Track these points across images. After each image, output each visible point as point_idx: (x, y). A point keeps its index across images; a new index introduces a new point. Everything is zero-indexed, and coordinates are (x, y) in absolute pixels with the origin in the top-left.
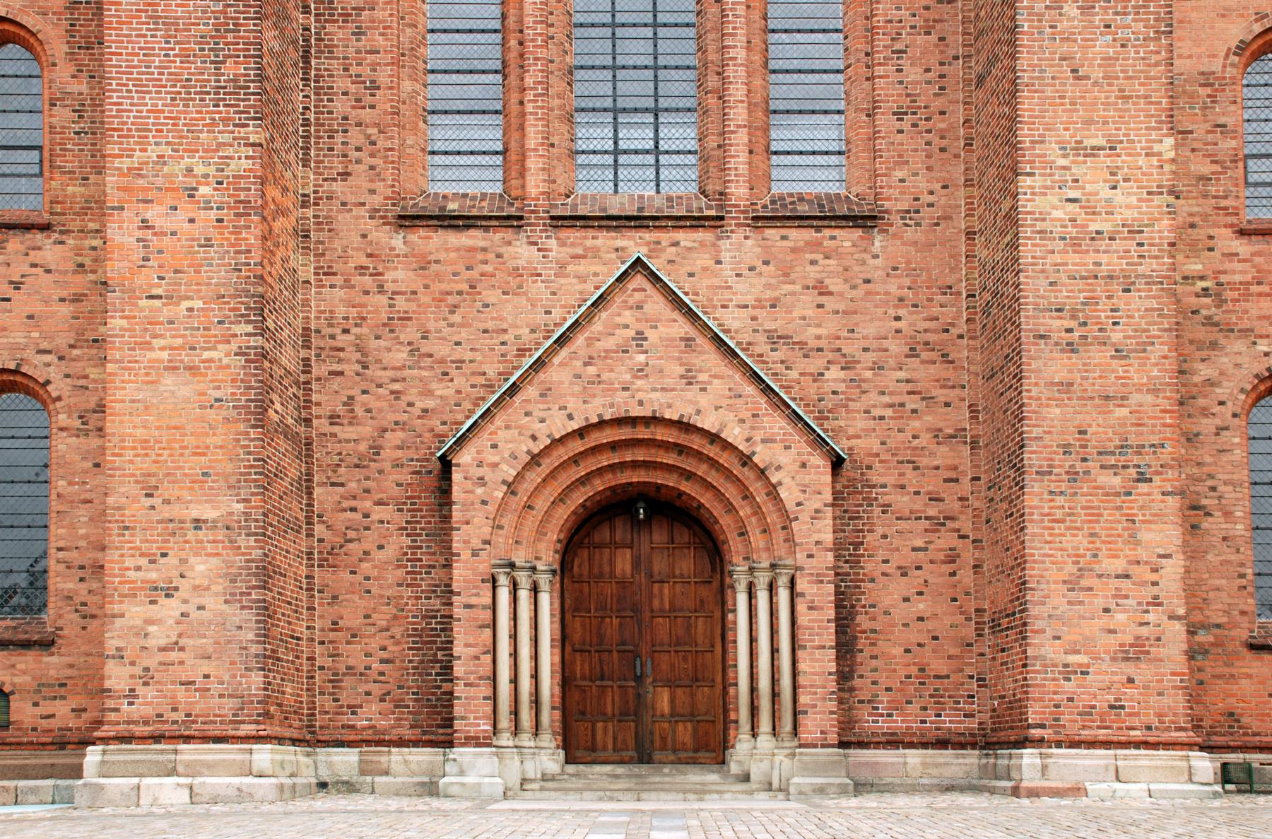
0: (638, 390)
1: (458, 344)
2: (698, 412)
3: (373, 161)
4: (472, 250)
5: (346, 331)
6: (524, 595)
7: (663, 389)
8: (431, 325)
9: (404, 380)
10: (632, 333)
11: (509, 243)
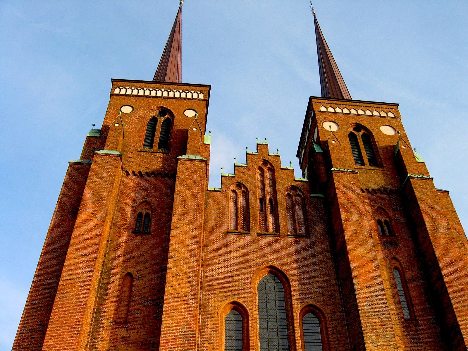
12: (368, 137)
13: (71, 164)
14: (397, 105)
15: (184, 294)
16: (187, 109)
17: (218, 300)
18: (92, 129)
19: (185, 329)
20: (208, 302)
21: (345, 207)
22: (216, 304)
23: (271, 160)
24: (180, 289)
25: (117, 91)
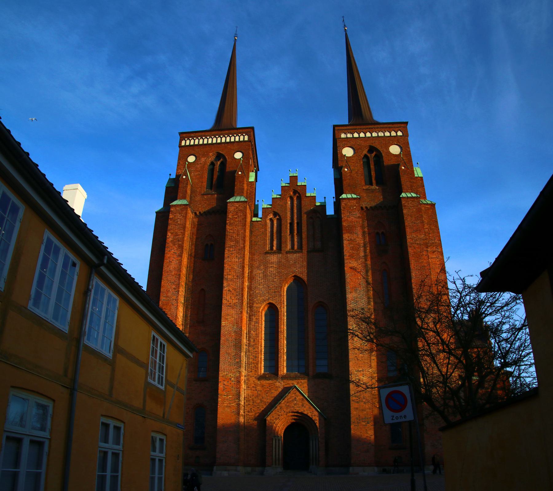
0: (295, 407)
1: (268, 399)
2: (304, 411)
3: (255, 369)
4: (270, 383)
5: (251, 397)
6: (277, 441)
7: (299, 407)
8: (264, 396)
9: (259, 405)
10: (294, 398)
11: (276, 382)
12: (379, 157)
13: (157, 213)
14: (406, 123)
15: (234, 303)
16: (236, 151)
17: (259, 303)
18: (170, 179)
19: (235, 327)
20: (253, 304)
21: (347, 229)
22: (258, 305)
23: (299, 189)
24: (232, 301)
25: (183, 143)
